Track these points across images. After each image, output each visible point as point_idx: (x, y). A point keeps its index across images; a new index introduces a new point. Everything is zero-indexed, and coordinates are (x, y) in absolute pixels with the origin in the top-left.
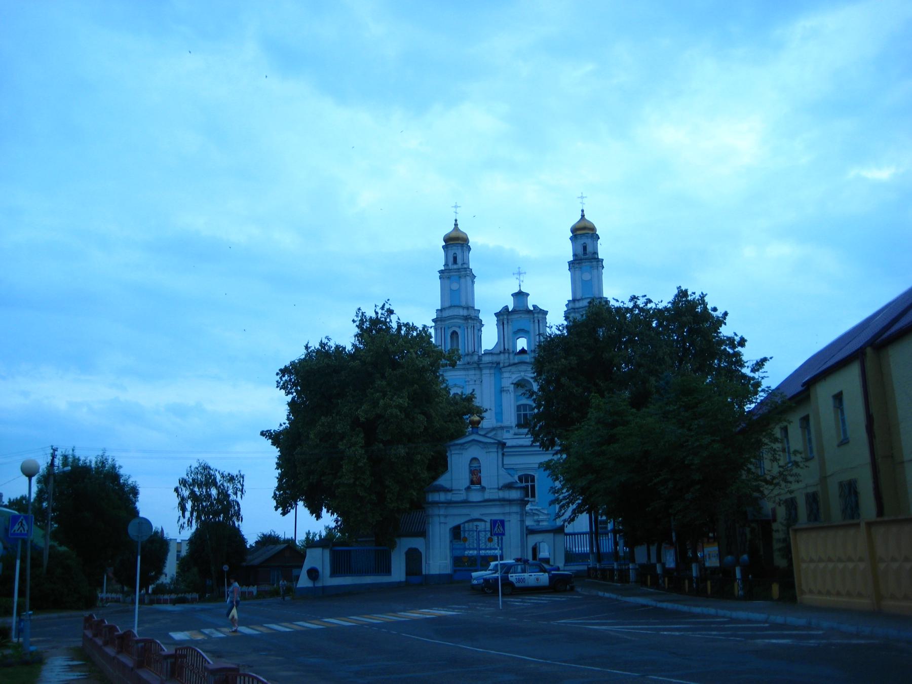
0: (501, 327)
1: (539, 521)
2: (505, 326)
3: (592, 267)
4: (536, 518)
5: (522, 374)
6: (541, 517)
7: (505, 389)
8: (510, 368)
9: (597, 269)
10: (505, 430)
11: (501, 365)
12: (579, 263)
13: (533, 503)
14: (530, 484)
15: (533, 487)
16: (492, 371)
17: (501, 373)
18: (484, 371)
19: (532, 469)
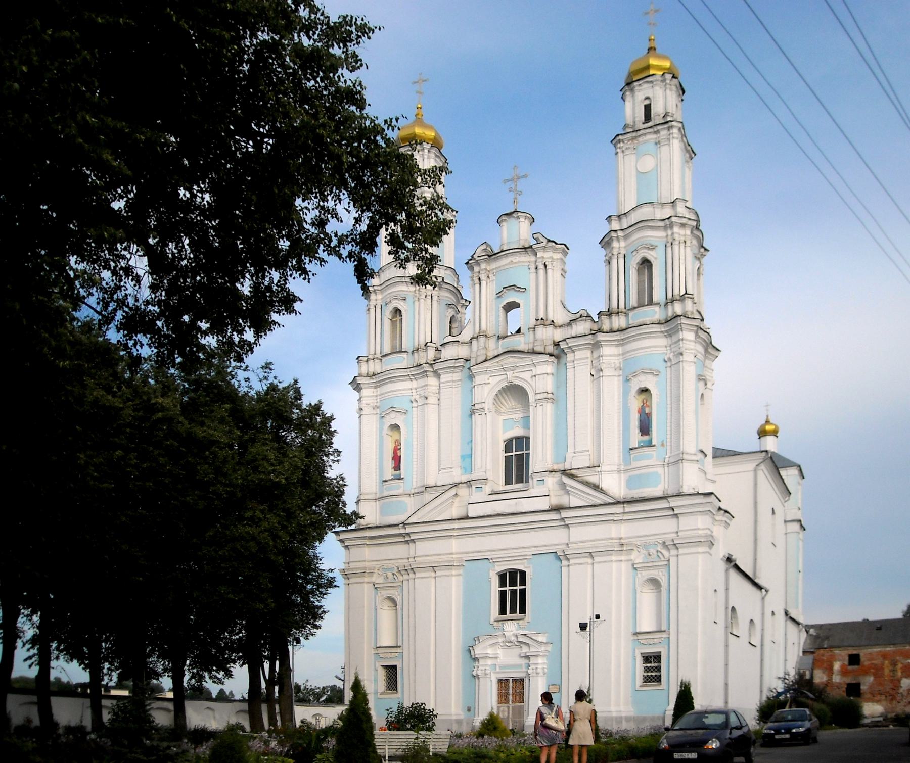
0: (477, 286)
1: (528, 657)
2: (483, 283)
3: (658, 143)
4: (525, 649)
5: (510, 374)
6: (532, 649)
7: (477, 407)
8: (487, 364)
9: (669, 145)
10: (474, 487)
11: (473, 362)
12: (633, 139)
13: (521, 622)
14: (518, 588)
15: (523, 592)
16: (457, 376)
17: (471, 377)
18: (444, 378)
19: (523, 558)
